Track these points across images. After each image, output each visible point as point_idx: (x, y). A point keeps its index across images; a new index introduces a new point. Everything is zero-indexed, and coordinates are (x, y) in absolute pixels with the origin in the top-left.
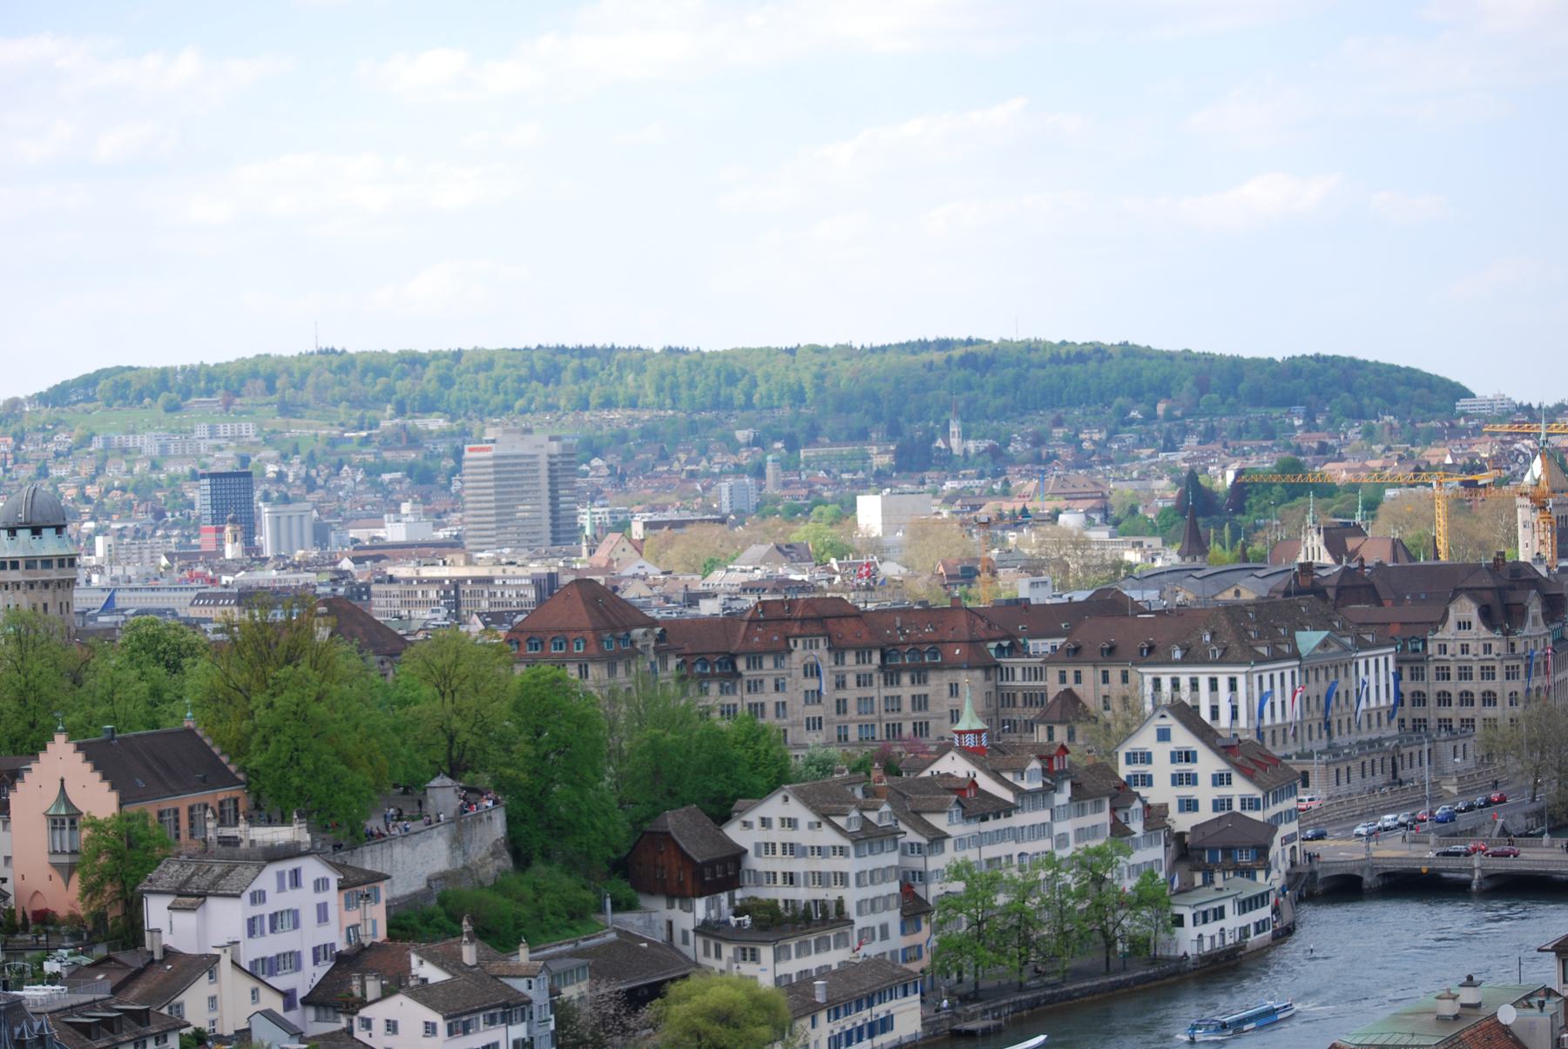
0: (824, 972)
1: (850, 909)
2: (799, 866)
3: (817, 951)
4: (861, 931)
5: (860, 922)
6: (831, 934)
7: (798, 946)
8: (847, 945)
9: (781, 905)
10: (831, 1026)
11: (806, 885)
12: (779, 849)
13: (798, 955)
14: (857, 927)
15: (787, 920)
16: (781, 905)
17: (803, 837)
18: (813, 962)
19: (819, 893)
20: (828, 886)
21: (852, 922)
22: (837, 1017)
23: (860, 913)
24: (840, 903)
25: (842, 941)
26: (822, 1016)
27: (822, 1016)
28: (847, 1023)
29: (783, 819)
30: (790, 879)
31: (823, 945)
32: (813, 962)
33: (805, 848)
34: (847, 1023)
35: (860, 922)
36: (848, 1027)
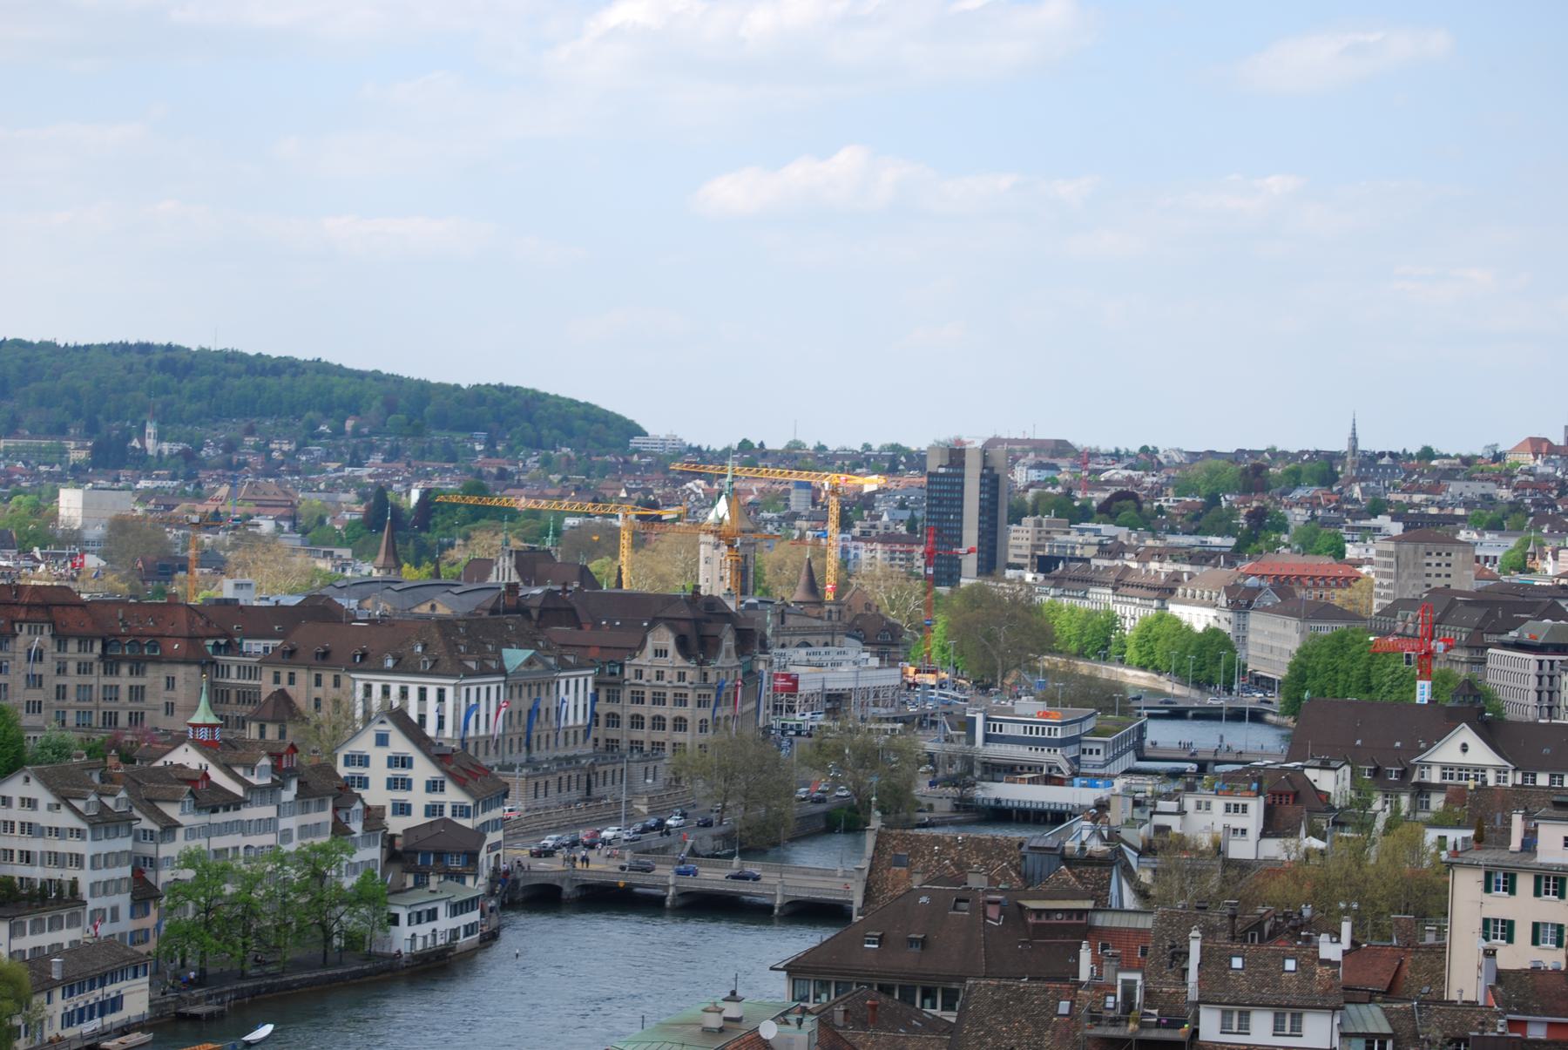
0: (56, 949)
1: (84, 889)
2: (36, 845)
3: (50, 930)
4: (93, 912)
5: (93, 904)
6: (65, 914)
7: (33, 923)
8: (79, 925)
9: (17, 881)
10: (65, 1003)
11: (42, 864)
12: (17, 827)
13: (32, 933)
14: (90, 908)
15: (23, 897)
16: (17, 881)
17: (42, 817)
18: (46, 939)
19: (55, 873)
20: (63, 866)
21: (85, 903)
22: (71, 995)
23: (92, 895)
24: (74, 884)
25: (75, 921)
26: (58, 993)
27: (58, 993)
28: (80, 1000)
29: (23, 799)
30: (27, 857)
31: (55, 924)
32: (46, 939)
33: (43, 828)
34: (80, 1000)
35: (93, 904)
36: (81, 1005)
